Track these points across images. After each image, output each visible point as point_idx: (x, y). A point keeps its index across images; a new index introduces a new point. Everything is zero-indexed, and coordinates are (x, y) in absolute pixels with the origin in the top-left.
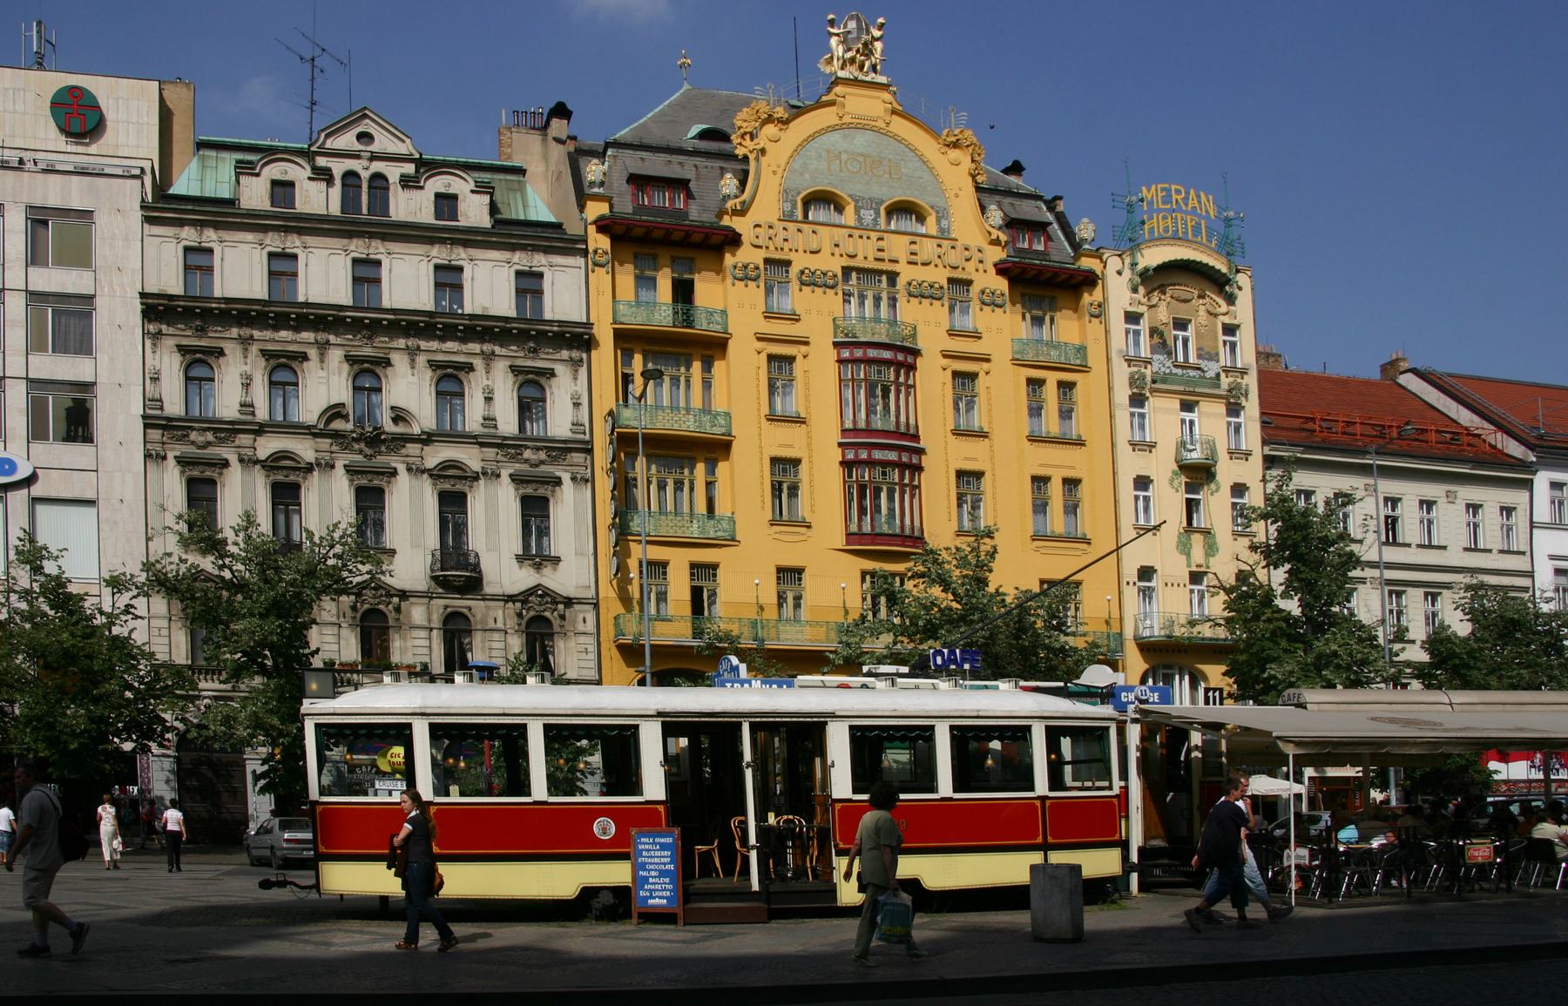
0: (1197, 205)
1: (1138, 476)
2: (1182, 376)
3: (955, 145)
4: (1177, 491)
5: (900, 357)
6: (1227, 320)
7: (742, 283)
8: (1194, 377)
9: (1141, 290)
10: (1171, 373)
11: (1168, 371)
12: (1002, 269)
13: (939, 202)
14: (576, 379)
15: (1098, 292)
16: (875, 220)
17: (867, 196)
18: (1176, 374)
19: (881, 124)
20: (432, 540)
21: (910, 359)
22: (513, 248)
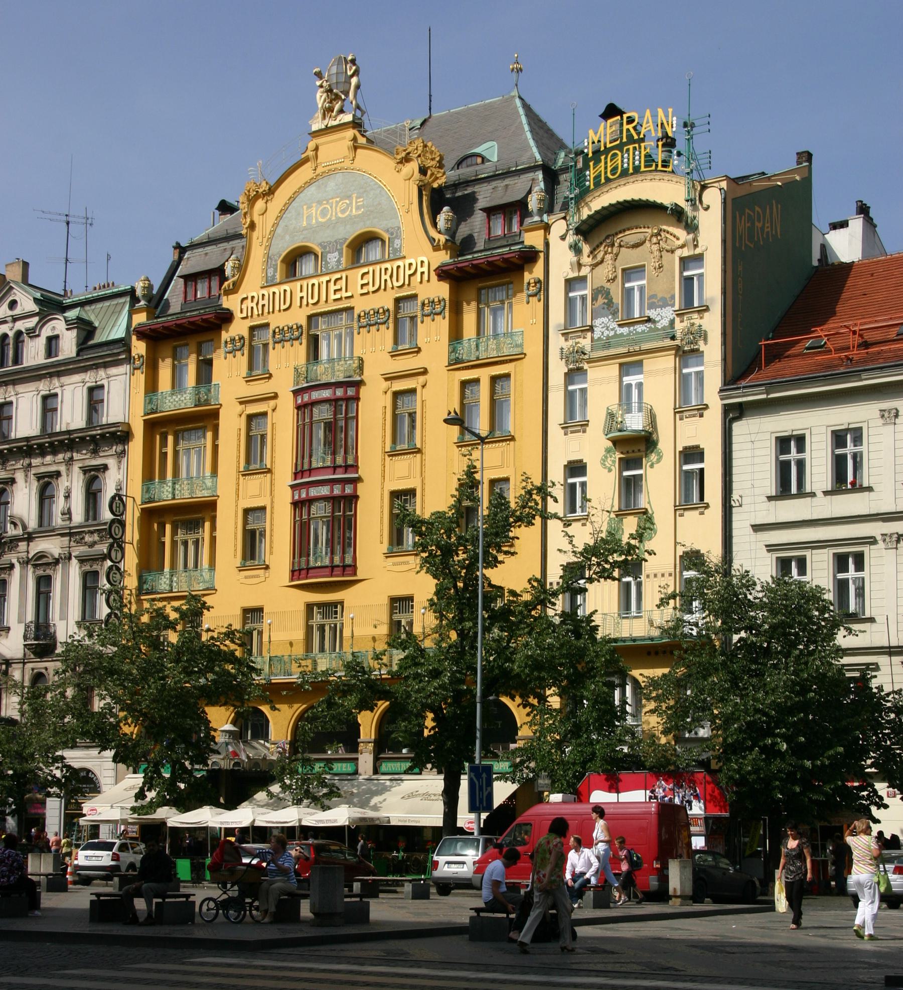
0: (652, 128)
1: (570, 462)
2: (628, 335)
3: (407, 159)
4: (610, 470)
5: (339, 392)
6: (686, 252)
7: (231, 355)
8: (643, 332)
9: (586, 249)
10: (616, 335)
11: (612, 333)
12: (443, 274)
13: (390, 224)
14: (119, 468)
15: (538, 271)
16: (339, 261)
17: (333, 240)
18: (622, 335)
19: (347, 163)
20: (30, 616)
21: (351, 392)
22: (85, 369)
